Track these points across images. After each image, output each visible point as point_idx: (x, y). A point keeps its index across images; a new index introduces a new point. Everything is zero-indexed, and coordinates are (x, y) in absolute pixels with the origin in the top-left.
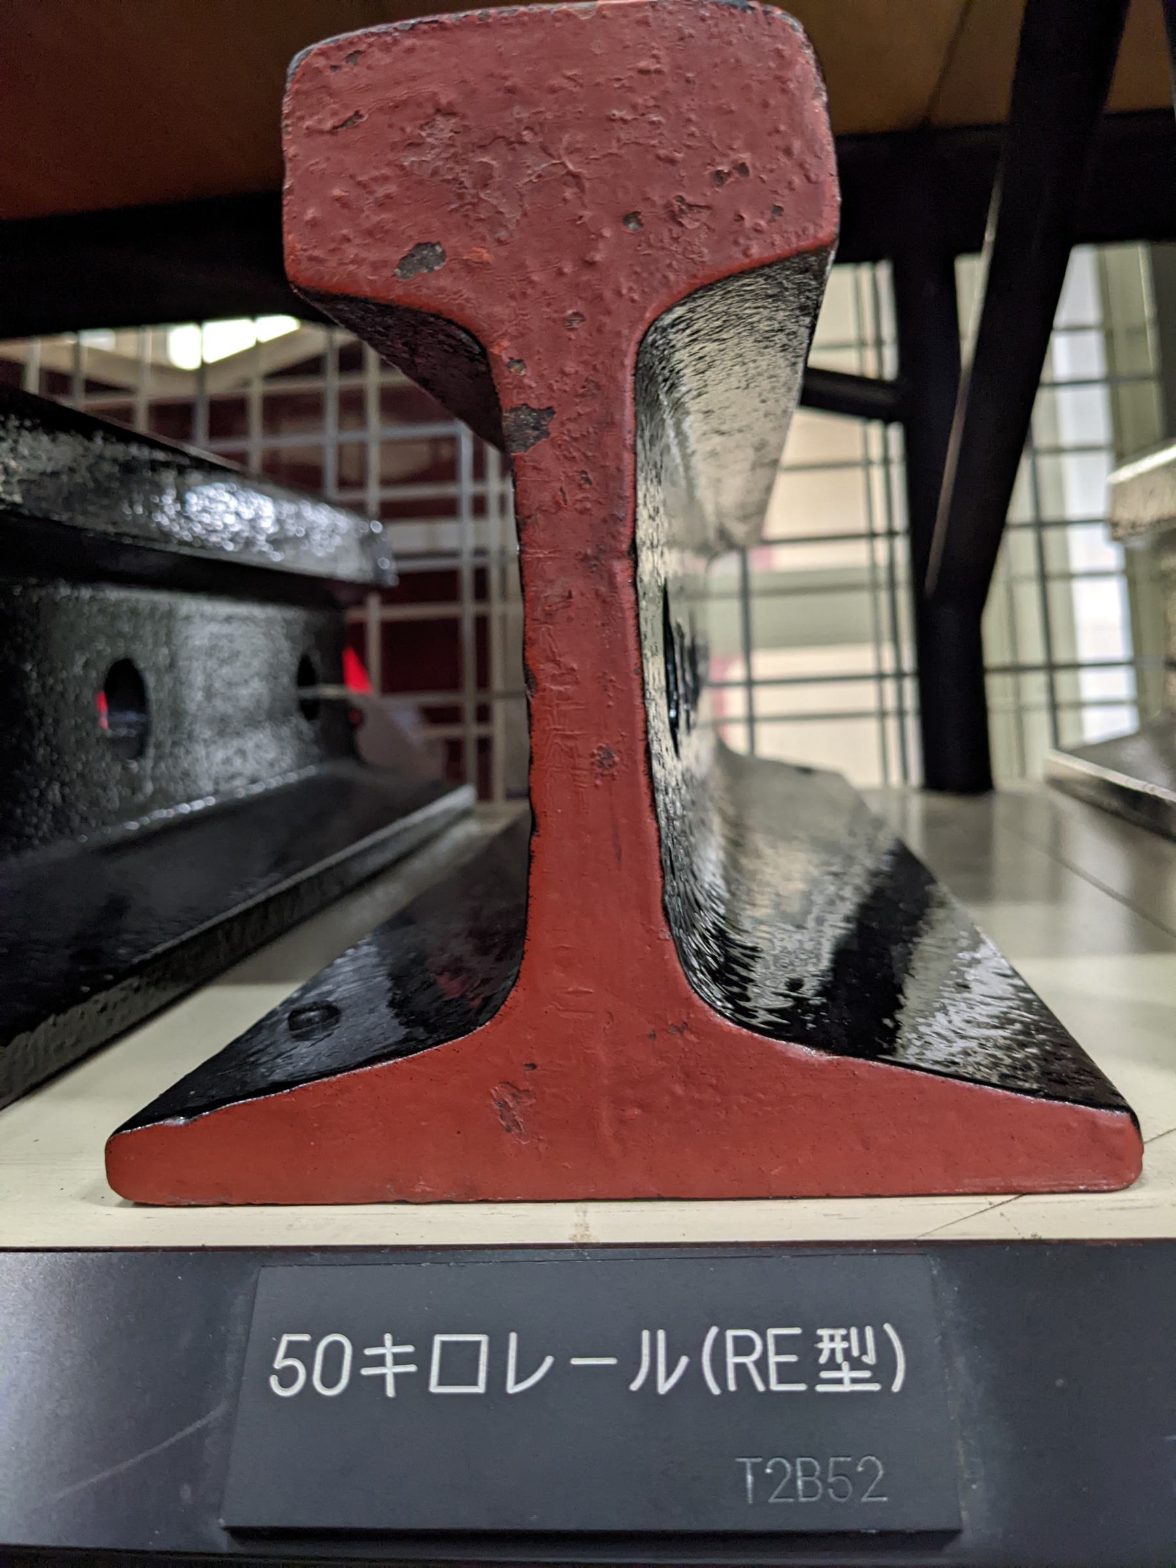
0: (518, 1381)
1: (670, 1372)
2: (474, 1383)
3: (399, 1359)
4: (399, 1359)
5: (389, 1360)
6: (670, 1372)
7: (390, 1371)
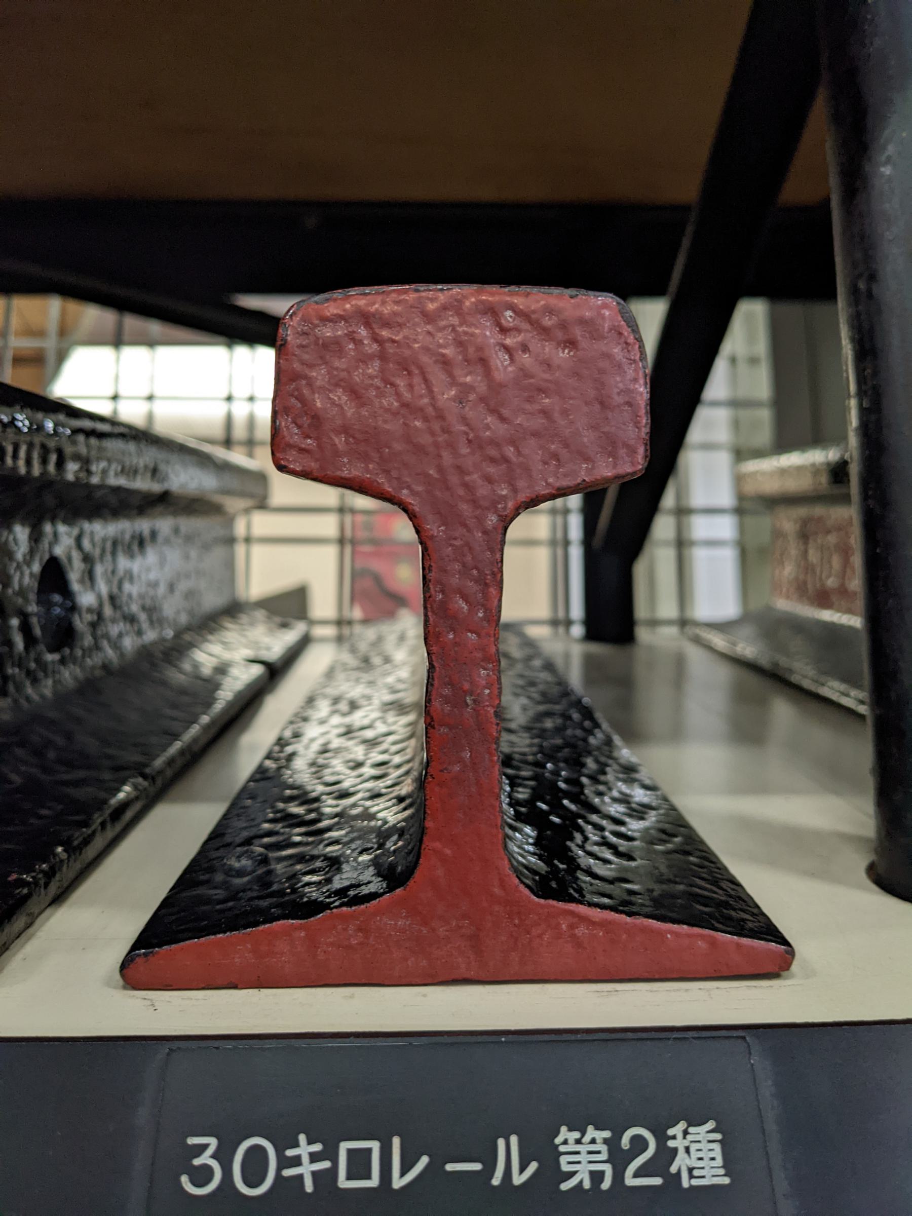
0: (403, 1174)
1: (522, 1170)
3: (314, 1158)
4: (314, 1158)
5: (305, 1159)
7: (306, 1169)
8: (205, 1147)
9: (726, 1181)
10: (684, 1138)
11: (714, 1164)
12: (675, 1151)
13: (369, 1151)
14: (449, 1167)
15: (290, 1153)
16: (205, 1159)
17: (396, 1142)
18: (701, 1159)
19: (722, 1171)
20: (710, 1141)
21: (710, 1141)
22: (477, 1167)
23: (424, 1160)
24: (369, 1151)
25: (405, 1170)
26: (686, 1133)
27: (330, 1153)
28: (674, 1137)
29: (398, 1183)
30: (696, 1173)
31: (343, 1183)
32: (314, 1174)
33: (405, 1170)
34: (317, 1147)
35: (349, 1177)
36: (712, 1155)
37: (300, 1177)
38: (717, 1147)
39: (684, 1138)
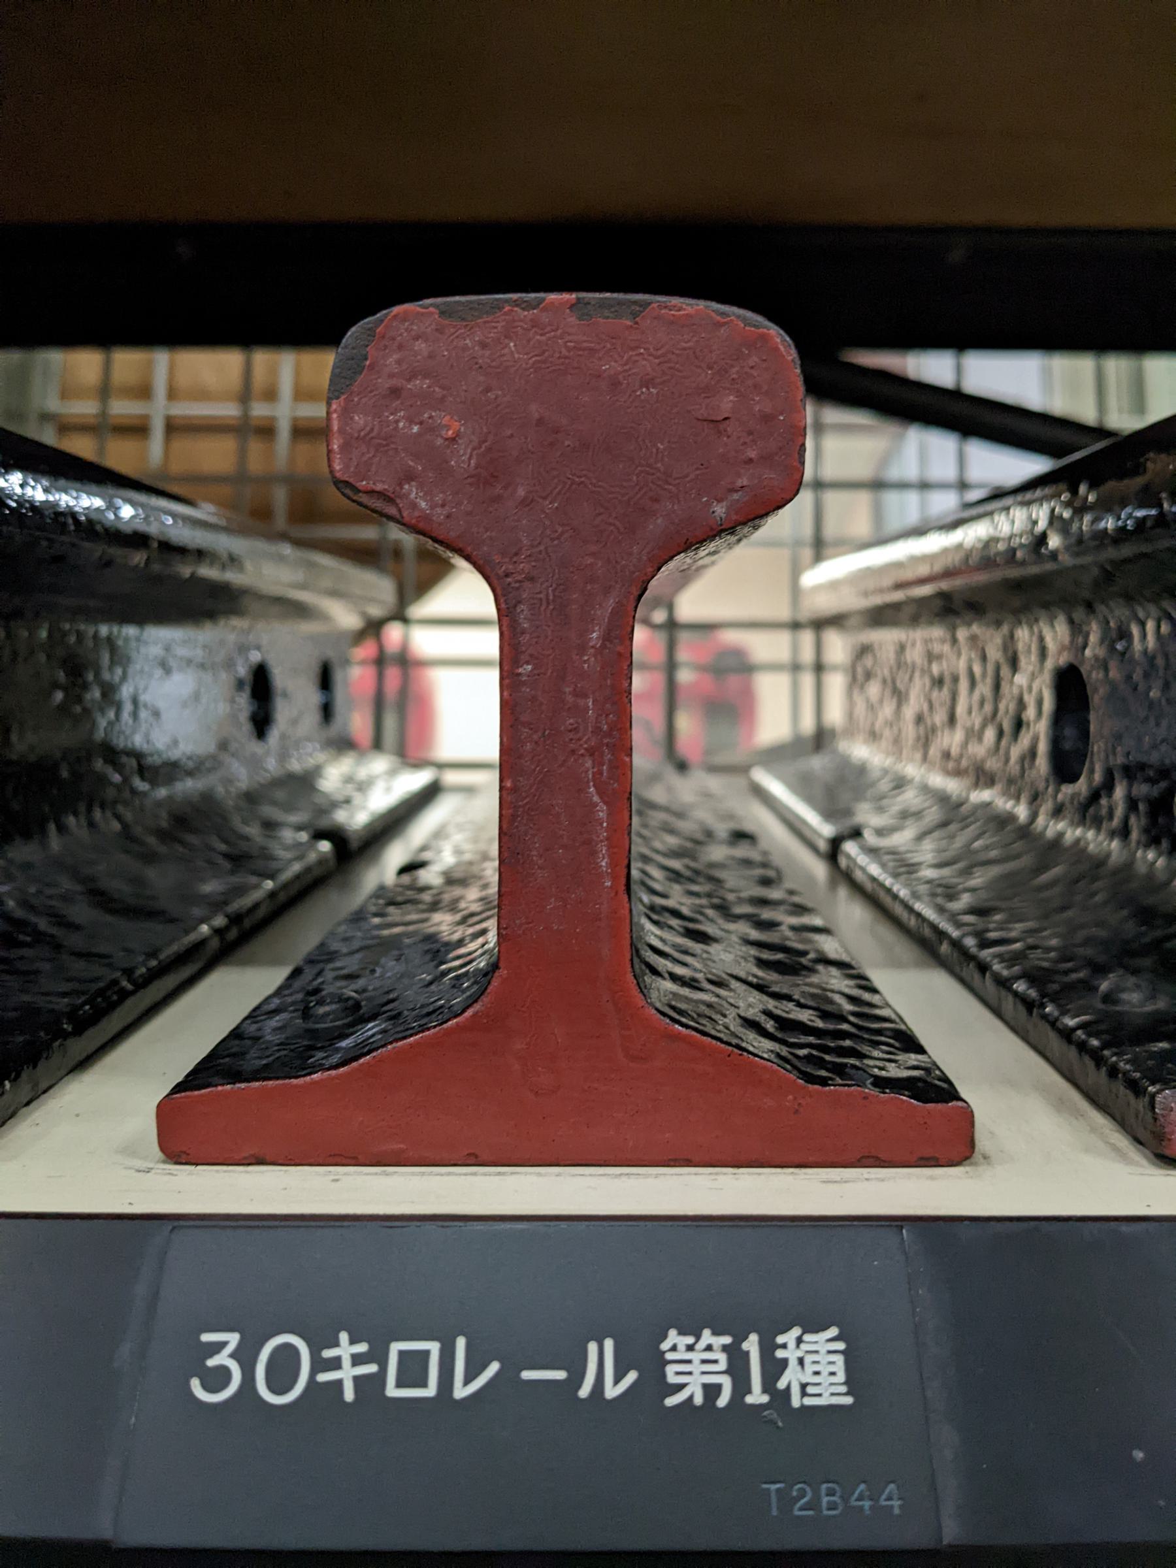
2: (424, 1384)
3: (357, 1360)
4: (357, 1360)
5: (346, 1362)
7: (347, 1374)
8: (223, 1345)
9: (848, 1400)
10: (798, 1346)
11: (833, 1379)
12: (784, 1363)
15: (328, 1353)
16: (221, 1359)
18: (817, 1373)
19: (844, 1389)
20: (830, 1352)
21: (830, 1352)
24: (426, 1354)
26: (799, 1341)
27: (378, 1355)
28: (784, 1346)
30: (810, 1390)
31: (392, 1391)
32: (356, 1379)
34: (362, 1348)
35: (400, 1384)
36: (832, 1368)
37: (339, 1383)
38: (839, 1359)
39: (798, 1346)
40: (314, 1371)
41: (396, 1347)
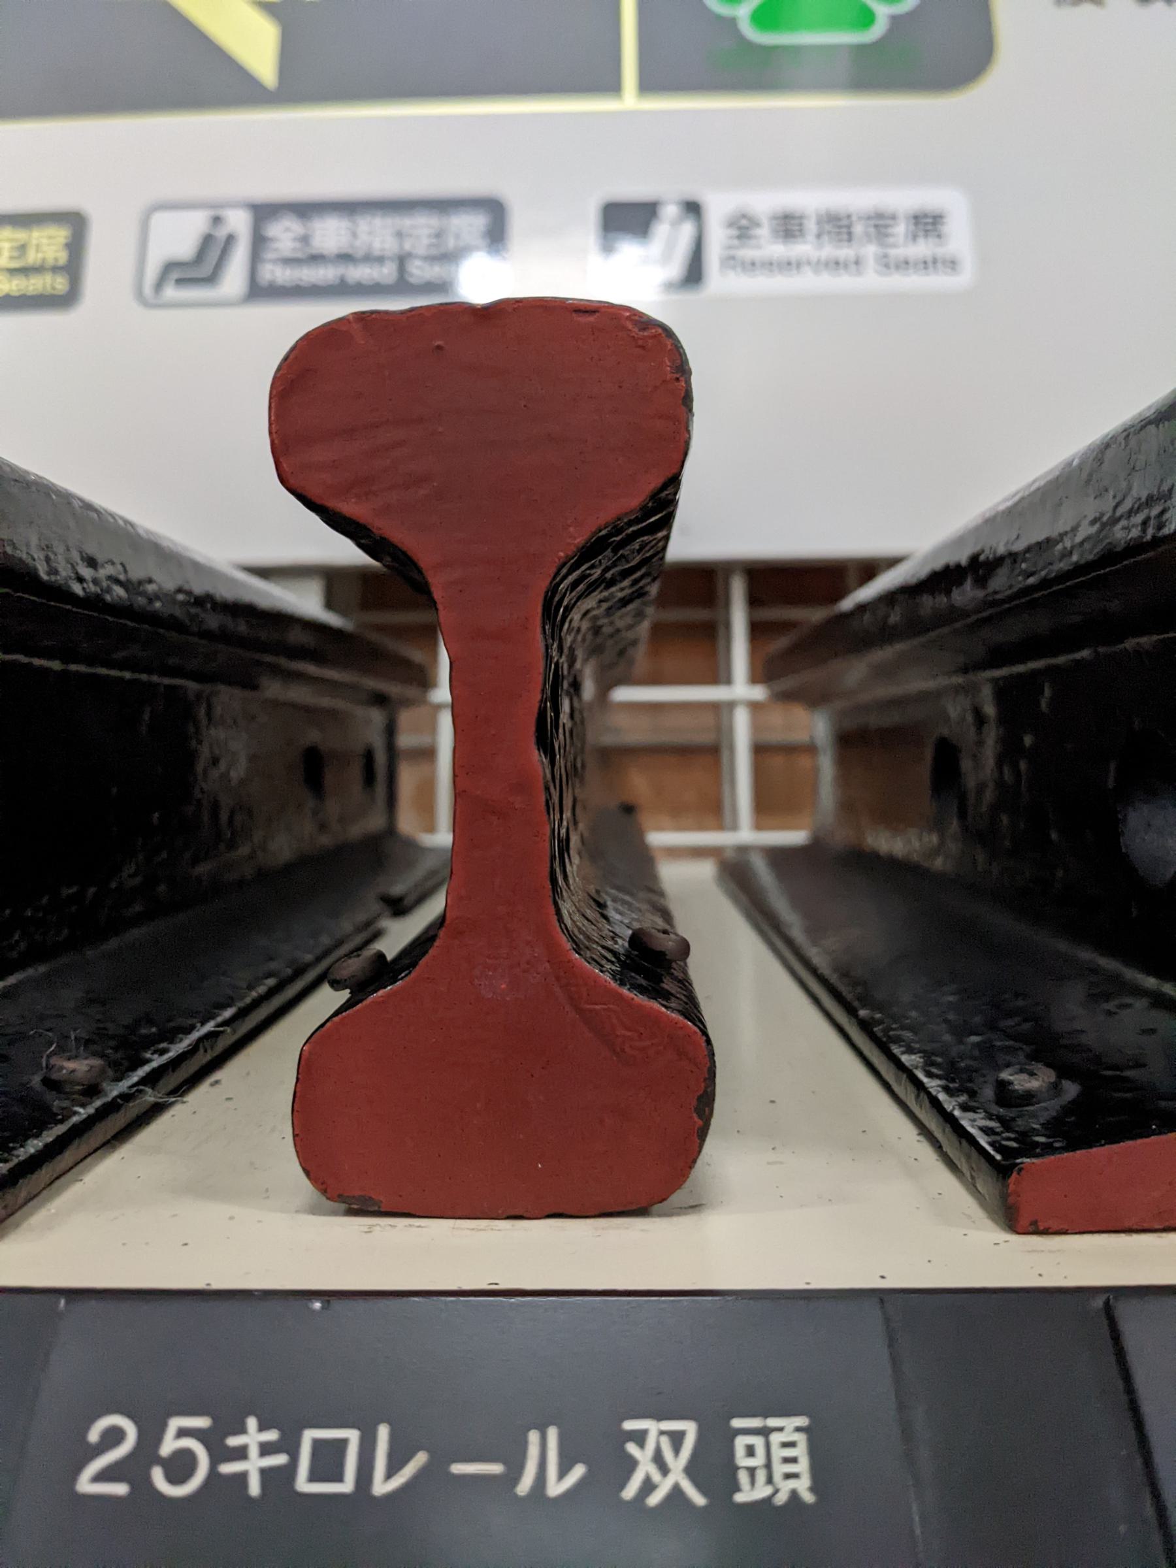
0: (389, 1475)
1: (563, 1473)
3: (266, 1449)
4: (266, 1449)
5: (254, 1451)
6: (563, 1473)
7: (253, 1466)
13: (343, 1443)
14: (458, 1468)
15: (233, 1441)
17: (383, 1432)
22: (496, 1468)
23: (421, 1458)
24: (343, 1443)
25: (392, 1470)
27: (289, 1445)
29: (381, 1487)
31: (303, 1484)
32: (264, 1473)
33: (392, 1470)
34: (272, 1436)
35: (313, 1477)
37: (242, 1477)
40: (214, 1463)
41: (309, 1436)
